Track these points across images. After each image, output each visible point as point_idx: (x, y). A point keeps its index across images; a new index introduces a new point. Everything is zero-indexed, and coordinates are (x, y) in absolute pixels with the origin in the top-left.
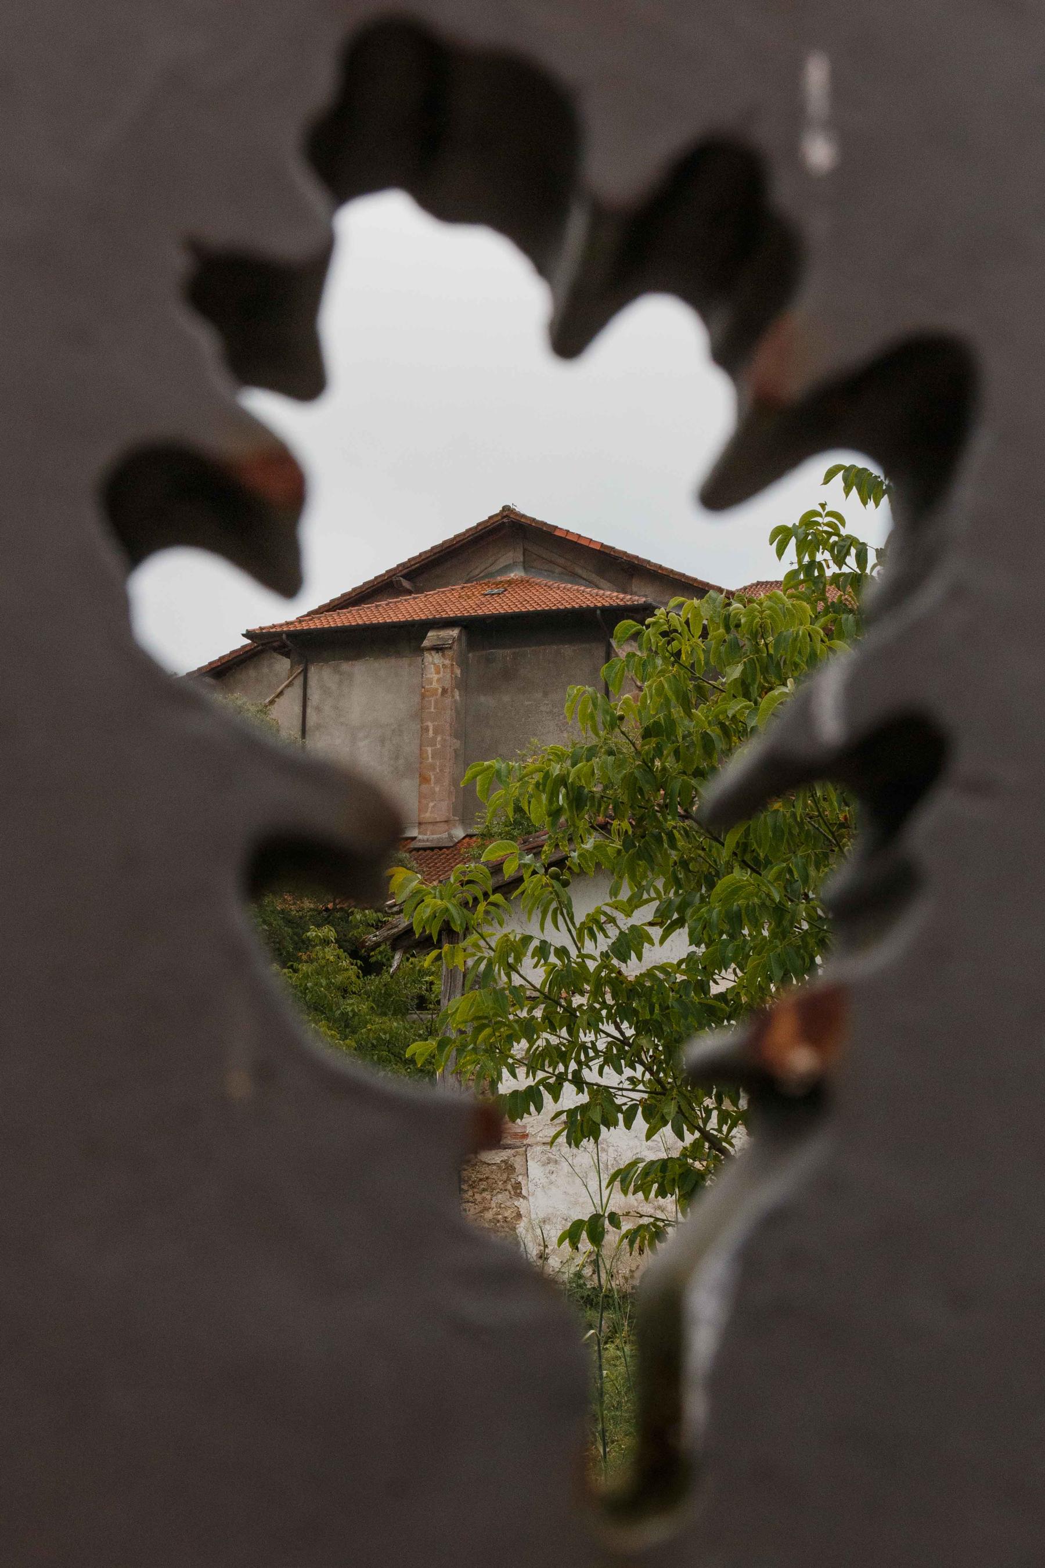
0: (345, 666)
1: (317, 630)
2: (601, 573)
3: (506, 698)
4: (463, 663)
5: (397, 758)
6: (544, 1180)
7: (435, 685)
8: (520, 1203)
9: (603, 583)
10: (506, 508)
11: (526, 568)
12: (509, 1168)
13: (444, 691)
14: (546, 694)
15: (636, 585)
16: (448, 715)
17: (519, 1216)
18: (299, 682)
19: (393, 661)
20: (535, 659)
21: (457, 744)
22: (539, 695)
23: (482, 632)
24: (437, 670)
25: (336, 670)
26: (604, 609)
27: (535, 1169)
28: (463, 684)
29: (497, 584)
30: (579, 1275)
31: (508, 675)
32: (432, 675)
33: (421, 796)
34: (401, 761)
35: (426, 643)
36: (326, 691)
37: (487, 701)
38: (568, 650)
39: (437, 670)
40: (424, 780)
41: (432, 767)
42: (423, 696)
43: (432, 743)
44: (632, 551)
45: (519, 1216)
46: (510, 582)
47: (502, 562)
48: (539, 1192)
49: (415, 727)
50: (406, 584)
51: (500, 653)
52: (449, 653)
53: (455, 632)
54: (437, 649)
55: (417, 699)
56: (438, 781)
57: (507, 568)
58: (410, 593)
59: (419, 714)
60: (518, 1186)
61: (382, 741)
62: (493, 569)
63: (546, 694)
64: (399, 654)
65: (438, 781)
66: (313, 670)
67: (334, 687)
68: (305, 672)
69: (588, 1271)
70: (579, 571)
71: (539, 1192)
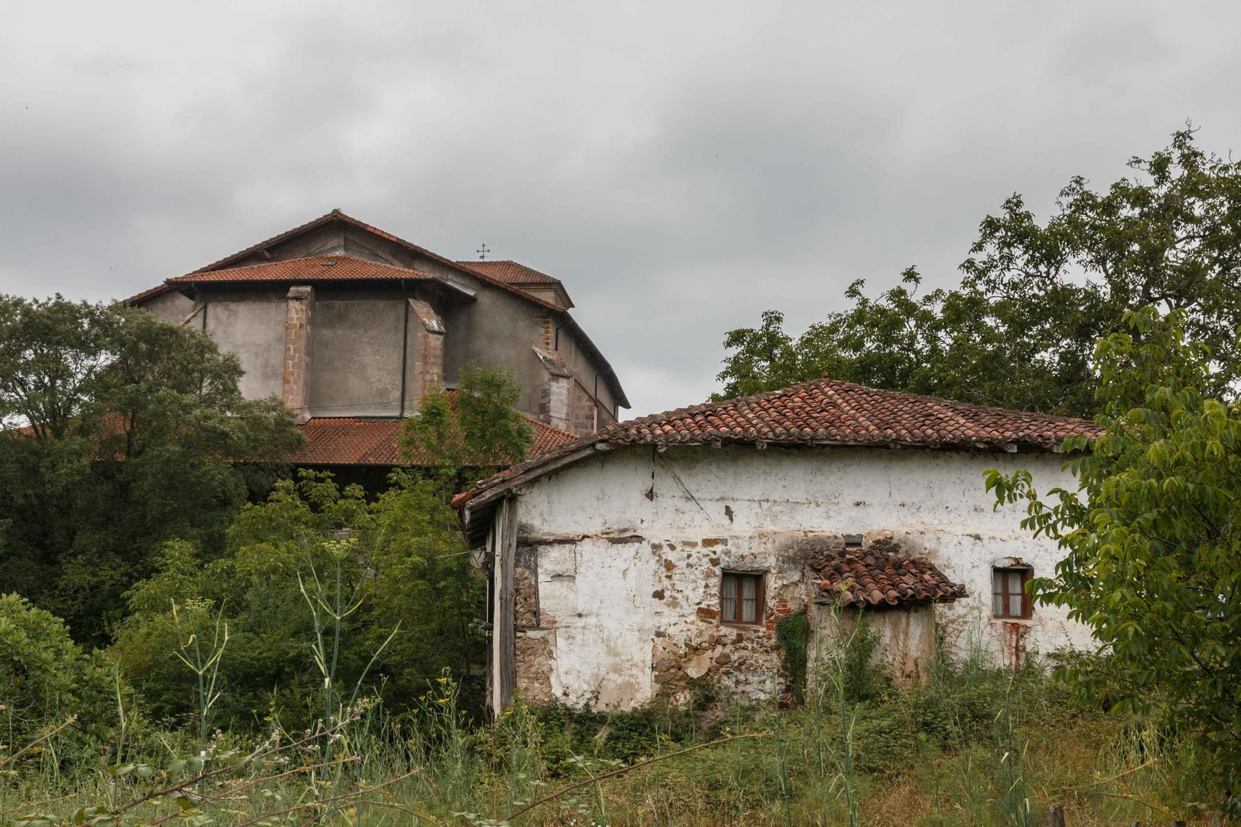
0: (233, 306)
1: (219, 282)
2: (394, 256)
3: (340, 332)
4: (312, 308)
5: (266, 366)
6: (566, 649)
7: (295, 321)
8: (552, 662)
9: (395, 262)
10: (335, 211)
11: (346, 248)
12: (545, 641)
13: (301, 326)
14: (366, 331)
15: (417, 265)
16: (303, 342)
17: (551, 670)
18: (201, 314)
19: (265, 305)
20: (360, 309)
21: (308, 359)
22: (361, 331)
23: (326, 290)
24: (296, 312)
25: (227, 308)
26: (406, 280)
27: (561, 642)
28: (312, 322)
29: (329, 259)
30: (587, 705)
31: (341, 317)
32: (293, 315)
33: (284, 392)
34: (269, 368)
35: (289, 295)
36: (219, 322)
37: (327, 333)
38: (381, 304)
39: (296, 312)
40: (286, 381)
41: (292, 374)
42: (287, 328)
43: (292, 358)
44: (266, 237)
45: (551, 670)
46: (337, 258)
47: (329, 246)
48: (563, 656)
49: (281, 347)
50: (267, 254)
51: (337, 303)
52: (305, 302)
53: (309, 289)
54: (297, 299)
55: (280, 329)
56: (295, 383)
57: (334, 249)
58: (268, 260)
59: (284, 340)
60: (551, 652)
61: (257, 355)
62: (326, 248)
63: (366, 331)
64: (268, 300)
65: (295, 383)
66: (210, 307)
67: (225, 318)
68: (205, 308)
69: (592, 703)
70: (380, 253)
71: (563, 656)
